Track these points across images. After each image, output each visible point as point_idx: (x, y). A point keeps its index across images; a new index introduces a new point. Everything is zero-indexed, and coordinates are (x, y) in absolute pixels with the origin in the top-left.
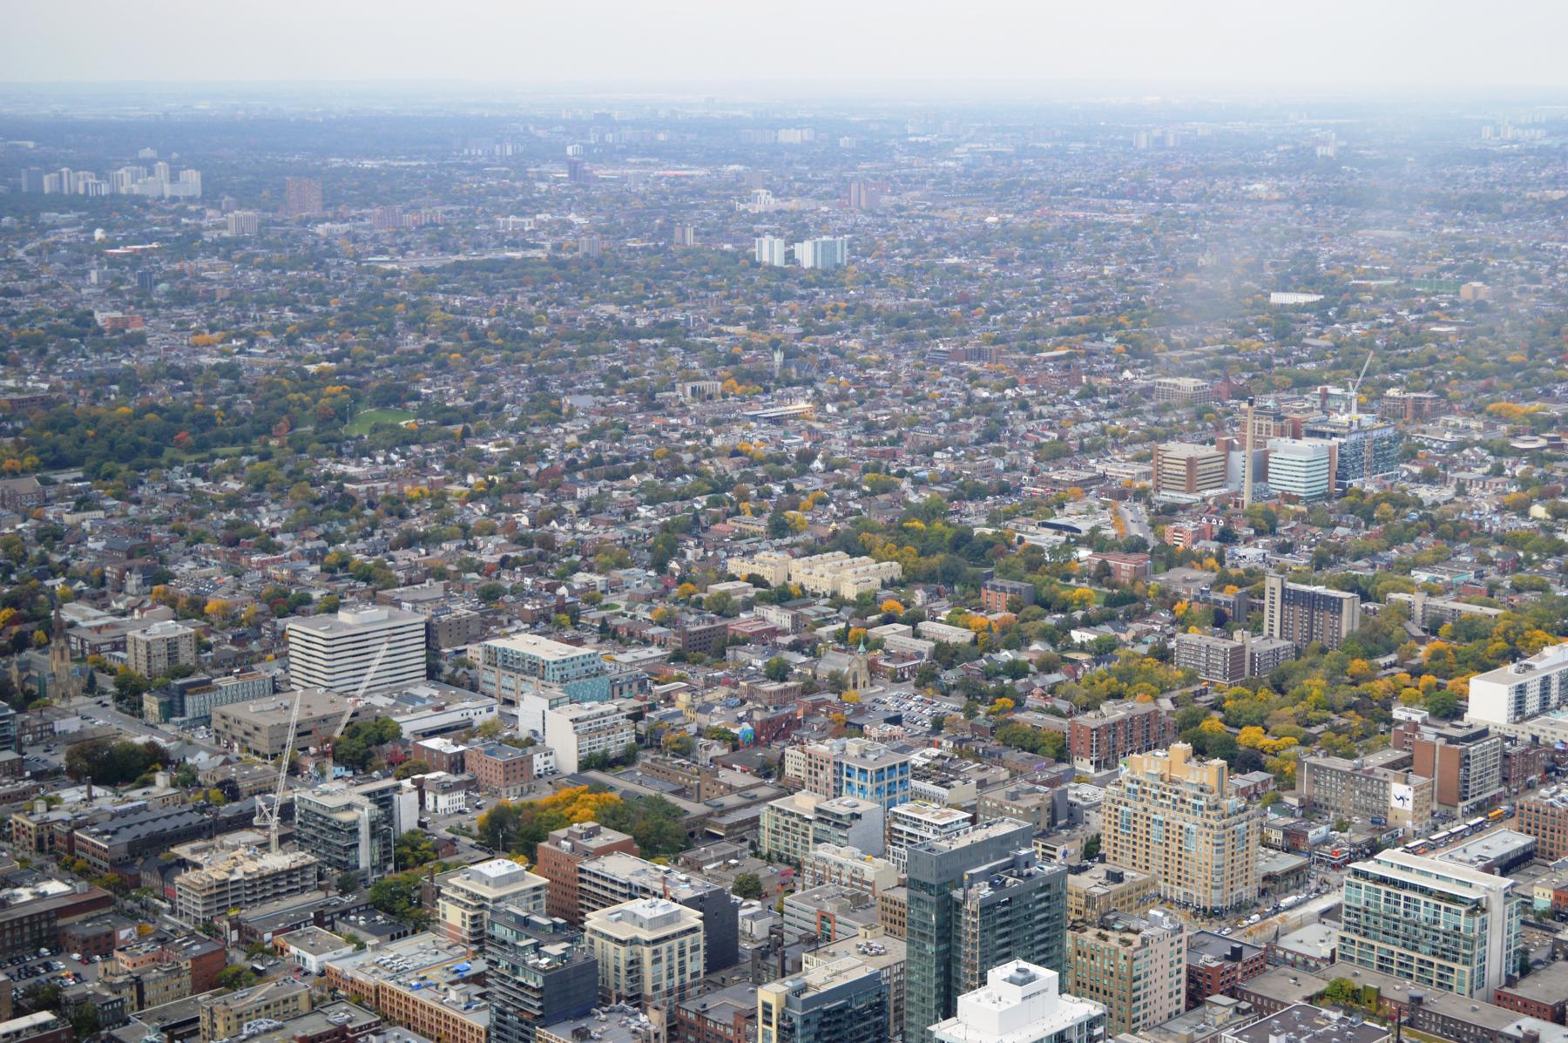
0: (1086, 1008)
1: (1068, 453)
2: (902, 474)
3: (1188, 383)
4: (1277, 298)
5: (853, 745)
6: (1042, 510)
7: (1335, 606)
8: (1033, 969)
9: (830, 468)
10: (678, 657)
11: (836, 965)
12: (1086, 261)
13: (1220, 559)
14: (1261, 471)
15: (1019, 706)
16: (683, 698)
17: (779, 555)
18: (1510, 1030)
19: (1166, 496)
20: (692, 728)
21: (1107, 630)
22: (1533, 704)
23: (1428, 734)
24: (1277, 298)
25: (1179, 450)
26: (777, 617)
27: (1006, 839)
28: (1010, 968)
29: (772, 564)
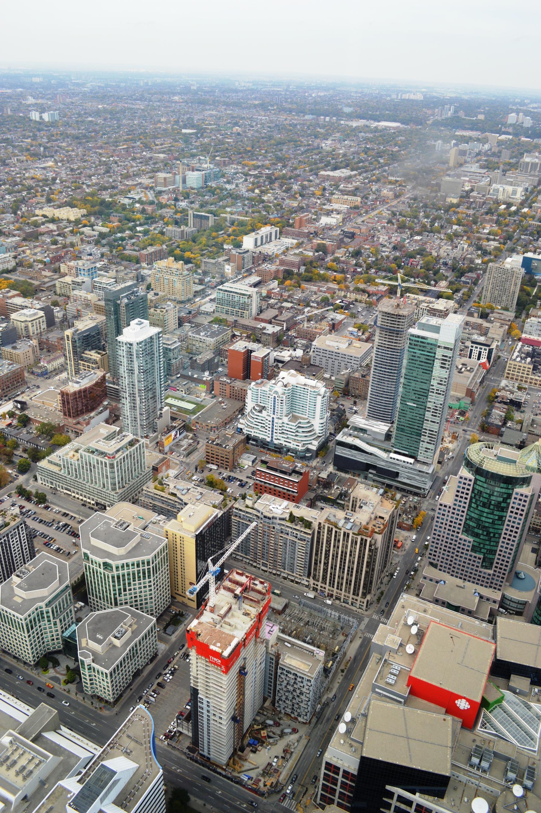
0: (157, 330)
1: (130, 176)
2: (83, 183)
3: (162, 156)
4: (184, 131)
5: (80, 263)
6: (124, 193)
7: (207, 218)
8: (143, 320)
9: (62, 182)
10: (25, 240)
11: (85, 323)
12: (129, 119)
13: (175, 206)
14: (184, 181)
15: (124, 249)
16: (28, 252)
17: (51, 209)
18: (259, 326)
19: (158, 189)
20: (32, 260)
21: (146, 227)
22: (259, 243)
23: (234, 252)
24: (184, 131)
25: (161, 175)
26: (52, 227)
27: (130, 286)
28: (137, 321)
29: (49, 211)
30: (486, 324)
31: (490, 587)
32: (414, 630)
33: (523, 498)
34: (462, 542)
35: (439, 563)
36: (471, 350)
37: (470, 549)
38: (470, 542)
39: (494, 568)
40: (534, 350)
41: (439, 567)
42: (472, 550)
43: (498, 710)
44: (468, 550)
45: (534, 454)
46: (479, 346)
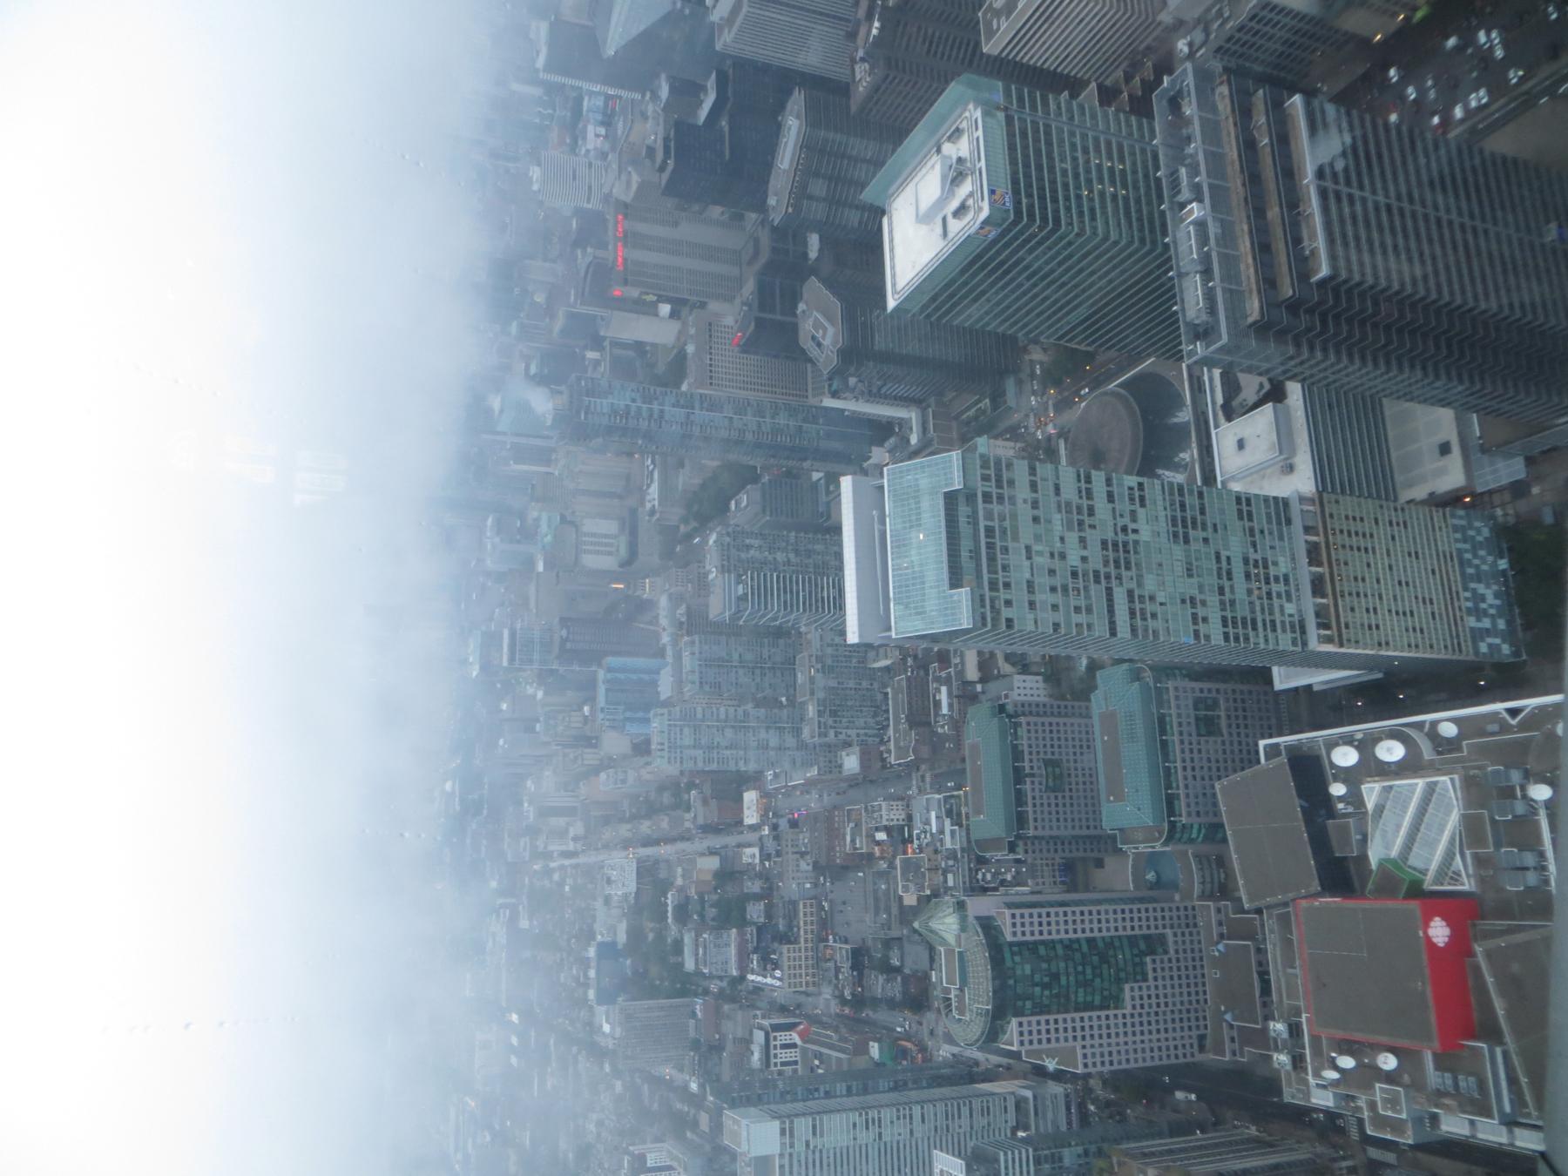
30: (729, 1046)
31: (1195, 925)
32: (1347, 1062)
33: (1018, 920)
34: (1138, 1002)
35: (1195, 1033)
36: (783, 1064)
37: (1144, 985)
38: (1132, 989)
39: (1160, 931)
40: (756, 950)
41: (1202, 1031)
42: (1145, 980)
43: (1414, 861)
44: (1148, 988)
45: (934, 925)
46: (772, 1052)
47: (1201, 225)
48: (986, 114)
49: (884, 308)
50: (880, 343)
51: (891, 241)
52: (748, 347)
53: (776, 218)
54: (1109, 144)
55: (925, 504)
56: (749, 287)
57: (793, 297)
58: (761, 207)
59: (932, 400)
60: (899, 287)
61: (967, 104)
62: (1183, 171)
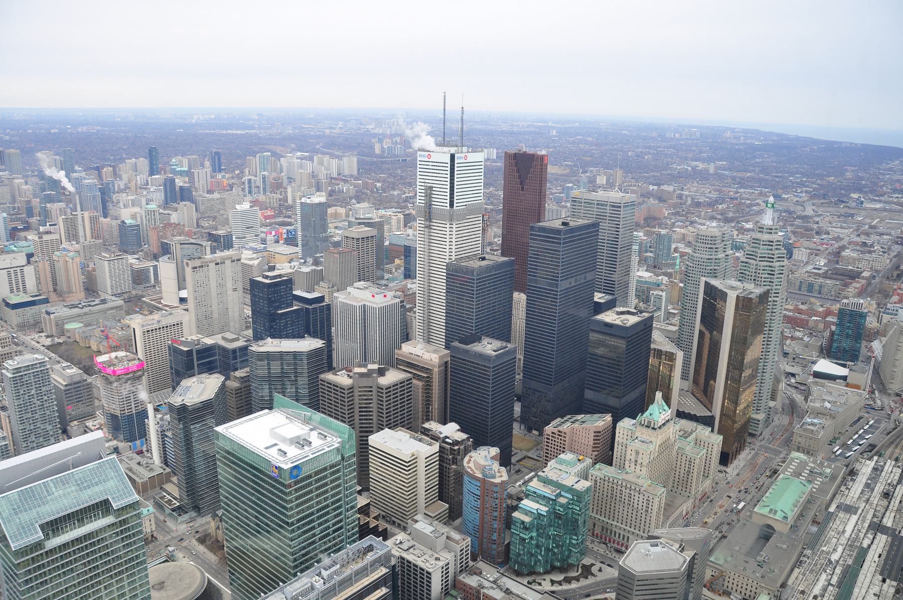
47: (312, 588)
48: (338, 449)
49: (217, 425)
50: (195, 428)
51: (256, 418)
52: (174, 351)
53: (254, 348)
54: (341, 521)
55: (97, 489)
56: (209, 341)
57: (209, 369)
58: (258, 337)
59: (168, 470)
60: (230, 430)
61: (340, 437)
62: (338, 566)
